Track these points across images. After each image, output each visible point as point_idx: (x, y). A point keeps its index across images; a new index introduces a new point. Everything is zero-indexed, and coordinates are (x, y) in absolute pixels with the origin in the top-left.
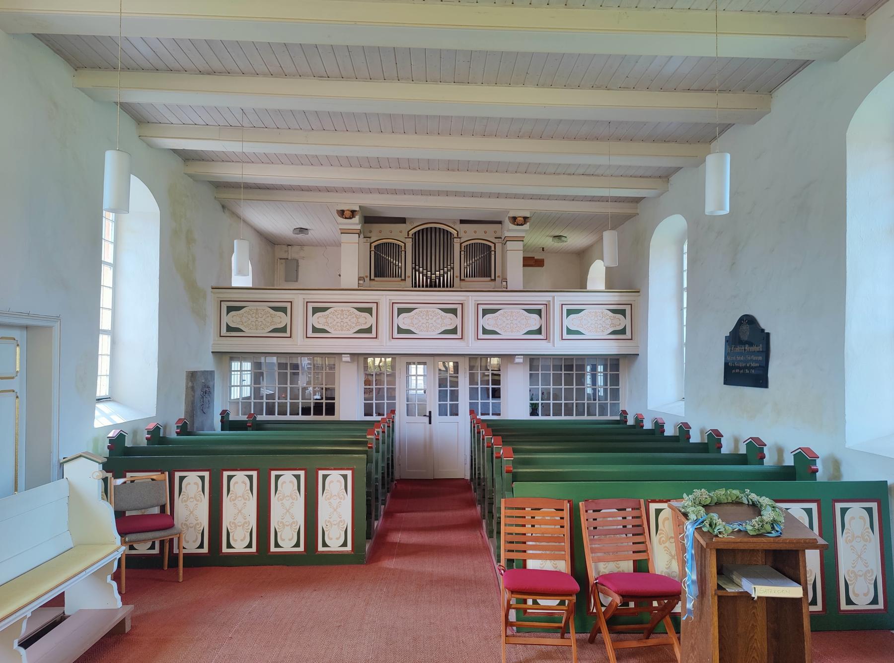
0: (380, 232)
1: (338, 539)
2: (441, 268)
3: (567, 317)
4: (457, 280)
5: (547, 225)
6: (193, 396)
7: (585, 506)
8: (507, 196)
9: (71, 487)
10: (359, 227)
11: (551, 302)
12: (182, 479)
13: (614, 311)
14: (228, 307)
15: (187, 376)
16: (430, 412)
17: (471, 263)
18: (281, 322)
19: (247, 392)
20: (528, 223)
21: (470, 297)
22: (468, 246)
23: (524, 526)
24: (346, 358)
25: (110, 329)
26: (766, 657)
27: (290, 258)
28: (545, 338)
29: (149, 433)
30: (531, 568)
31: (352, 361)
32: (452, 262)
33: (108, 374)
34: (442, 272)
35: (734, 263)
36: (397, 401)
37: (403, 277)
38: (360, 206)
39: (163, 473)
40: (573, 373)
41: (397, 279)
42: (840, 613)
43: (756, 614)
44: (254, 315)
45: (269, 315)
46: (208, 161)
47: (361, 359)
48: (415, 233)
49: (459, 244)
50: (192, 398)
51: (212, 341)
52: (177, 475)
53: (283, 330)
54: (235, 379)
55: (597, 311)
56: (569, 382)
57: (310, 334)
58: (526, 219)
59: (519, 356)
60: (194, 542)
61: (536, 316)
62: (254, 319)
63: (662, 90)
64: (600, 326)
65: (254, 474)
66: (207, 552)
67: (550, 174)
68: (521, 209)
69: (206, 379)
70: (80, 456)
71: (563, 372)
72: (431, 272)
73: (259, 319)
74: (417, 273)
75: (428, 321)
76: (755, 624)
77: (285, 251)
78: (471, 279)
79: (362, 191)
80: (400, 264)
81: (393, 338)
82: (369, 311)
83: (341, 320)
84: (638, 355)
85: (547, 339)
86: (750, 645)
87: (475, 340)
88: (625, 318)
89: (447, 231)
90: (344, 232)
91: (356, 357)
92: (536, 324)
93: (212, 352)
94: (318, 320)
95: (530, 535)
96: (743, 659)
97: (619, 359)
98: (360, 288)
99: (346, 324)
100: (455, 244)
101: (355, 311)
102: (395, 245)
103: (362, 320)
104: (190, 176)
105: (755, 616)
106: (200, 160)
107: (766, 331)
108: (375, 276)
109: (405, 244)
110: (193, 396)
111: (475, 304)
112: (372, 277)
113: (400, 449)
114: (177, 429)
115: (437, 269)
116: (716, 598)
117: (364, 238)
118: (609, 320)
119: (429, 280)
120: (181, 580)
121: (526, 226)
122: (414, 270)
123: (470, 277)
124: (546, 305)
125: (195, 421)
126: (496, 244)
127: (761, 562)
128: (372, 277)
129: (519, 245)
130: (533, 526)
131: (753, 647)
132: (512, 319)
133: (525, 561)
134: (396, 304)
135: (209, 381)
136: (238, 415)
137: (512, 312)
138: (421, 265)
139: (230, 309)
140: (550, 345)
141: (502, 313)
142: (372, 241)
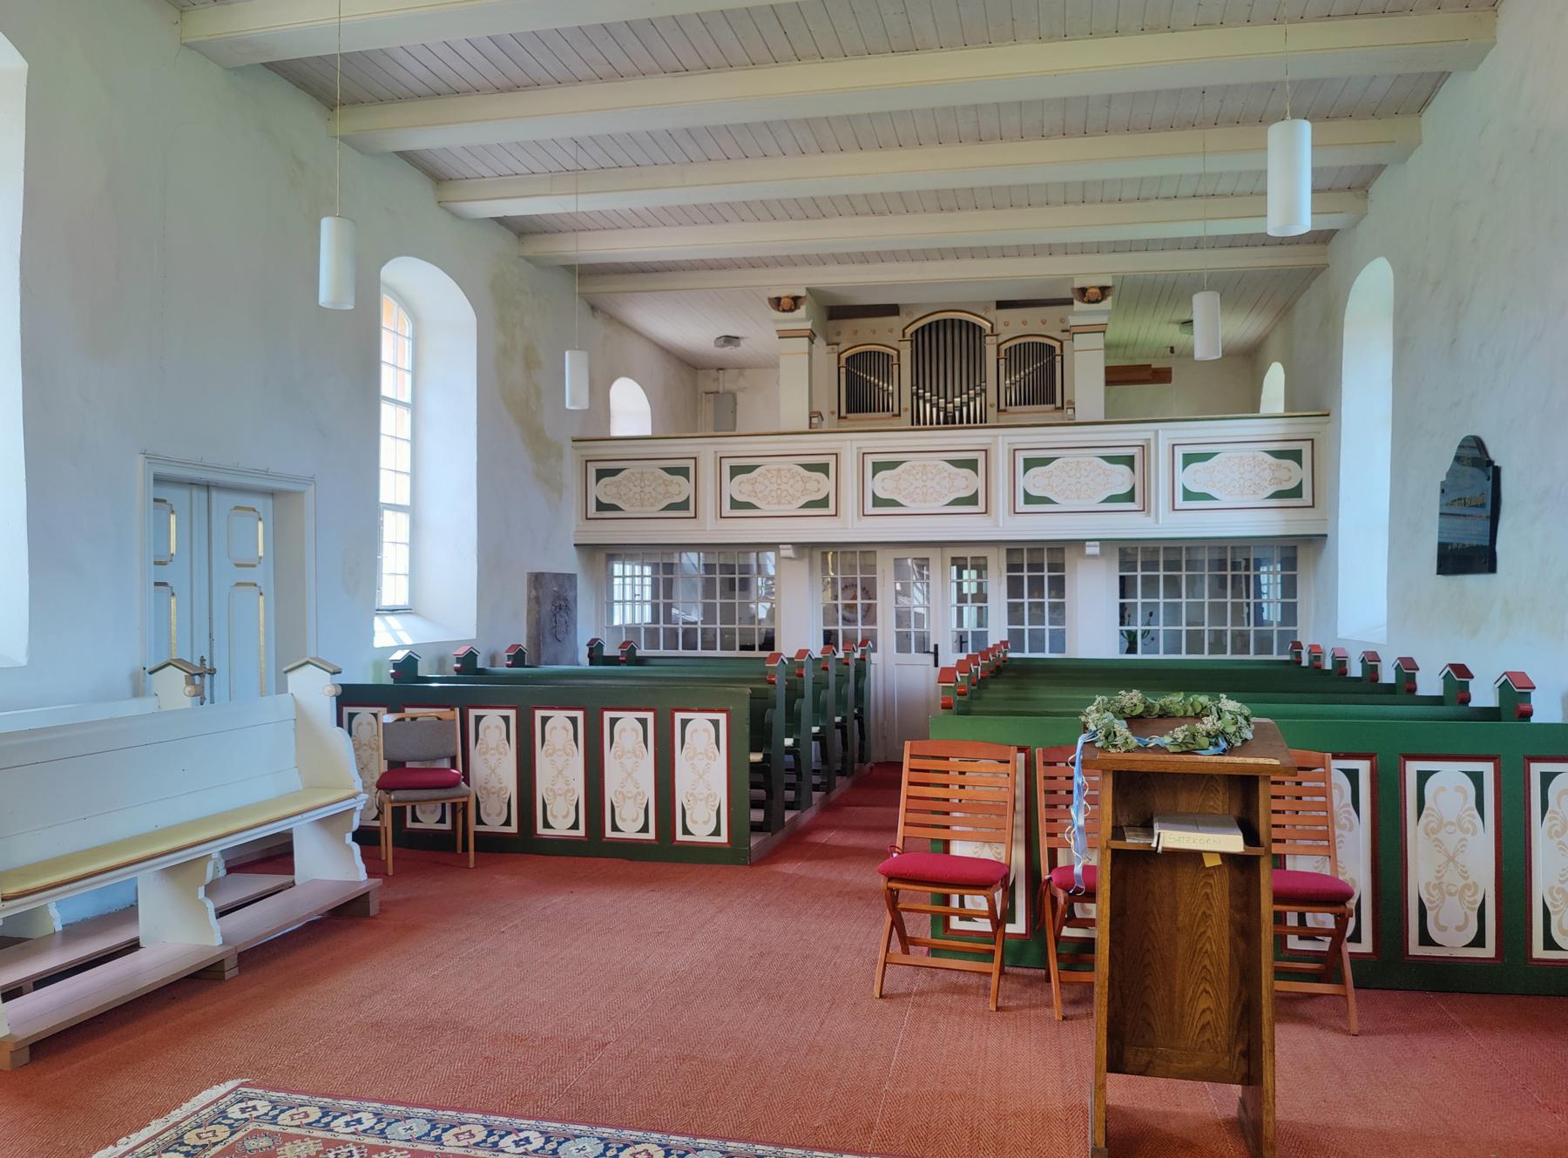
0: (856, 332)
1: (705, 823)
2: (964, 390)
3: (1183, 469)
4: (992, 412)
5: (1158, 300)
6: (539, 612)
7: (1044, 755)
8: (1067, 249)
9: (299, 709)
10: (808, 325)
11: (1152, 442)
12: (479, 719)
13: (1279, 454)
14: (598, 471)
15: (529, 580)
16: (936, 647)
17: (1018, 379)
18: (680, 493)
20: (1110, 299)
21: (1000, 438)
22: (1013, 350)
23: (947, 786)
24: (787, 552)
25: (409, 504)
26: (1227, 968)
27: (721, 391)
28: (1141, 509)
29: (458, 660)
30: (958, 855)
31: (799, 557)
32: (983, 380)
33: (407, 572)
34: (965, 396)
35: (1454, 340)
37: (896, 411)
38: (808, 289)
39: (452, 710)
41: (886, 414)
42: (1531, 963)
43: (1210, 896)
45: (660, 481)
46: (552, 232)
47: (817, 554)
48: (917, 331)
50: (537, 616)
51: (572, 527)
52: (473, 713)
53: (684, 505)
57: (727, 510)
58: (1104, 291)
59: (1092, 543)
60: (499, 814)
61: (1124, 469)
62: (639, 489)
63: (1276, 22)
65: (579, 715)
66: (516, 831)
67: (1130, 201)
68: (1093, 272)
69: (561, 586)
70: (308, 663)
72: (946, 398)
74: (921, 402)
76: (1208, 912)
78: (1018, 408)
79: (807, 260)
80: (890, 388)
81: (864, 515)
82: (824, 468)
83: (781, 487)
84: (1326, 536)
85: (1144, 510)
86: (1199, 947)
87: (1009, 515)
88: (1301, 467)
89: (974, 325)
90: (783, 335)
91: (806, 551)
93: (575, 545)
94: (739, 488)
95: (957, 801)
96: (1187, 969)
97: (1295, 547)
98: (811, 430)
101: (801, 470)
102: (881, 355)
103: (812, 486)
104: (528, 259)
105: (1208, 898)
106: (541, 233)
107: (1496, 464)
108: (849, 411)
109: (899, 352)
110: (539, 612)
111: (1009, 450)
112: (843, 413)
113: (885, 707)
114: (508, 660)
116: (1109, 853)
117: (828, 345)
118: (1268, 470)
119: (942, 414)
120: (472, 865)
121: (1107, 304)
122: (915, 397)
123: (1016, 404)
124: (1143, 446)
125: (542, 651)
126: (1065, 343)
127: (1220, 810)
128: (843, 413)
129: (1098, 340)
130: (962, 787)
131: (1204, 951)
132: (1078, 475)
133: (947, 843)
134: (869, 455)
135: (566, 590)
137: (1078, 462)
138: (927, 388)
139: (601, 474)
140: (1150, 520)
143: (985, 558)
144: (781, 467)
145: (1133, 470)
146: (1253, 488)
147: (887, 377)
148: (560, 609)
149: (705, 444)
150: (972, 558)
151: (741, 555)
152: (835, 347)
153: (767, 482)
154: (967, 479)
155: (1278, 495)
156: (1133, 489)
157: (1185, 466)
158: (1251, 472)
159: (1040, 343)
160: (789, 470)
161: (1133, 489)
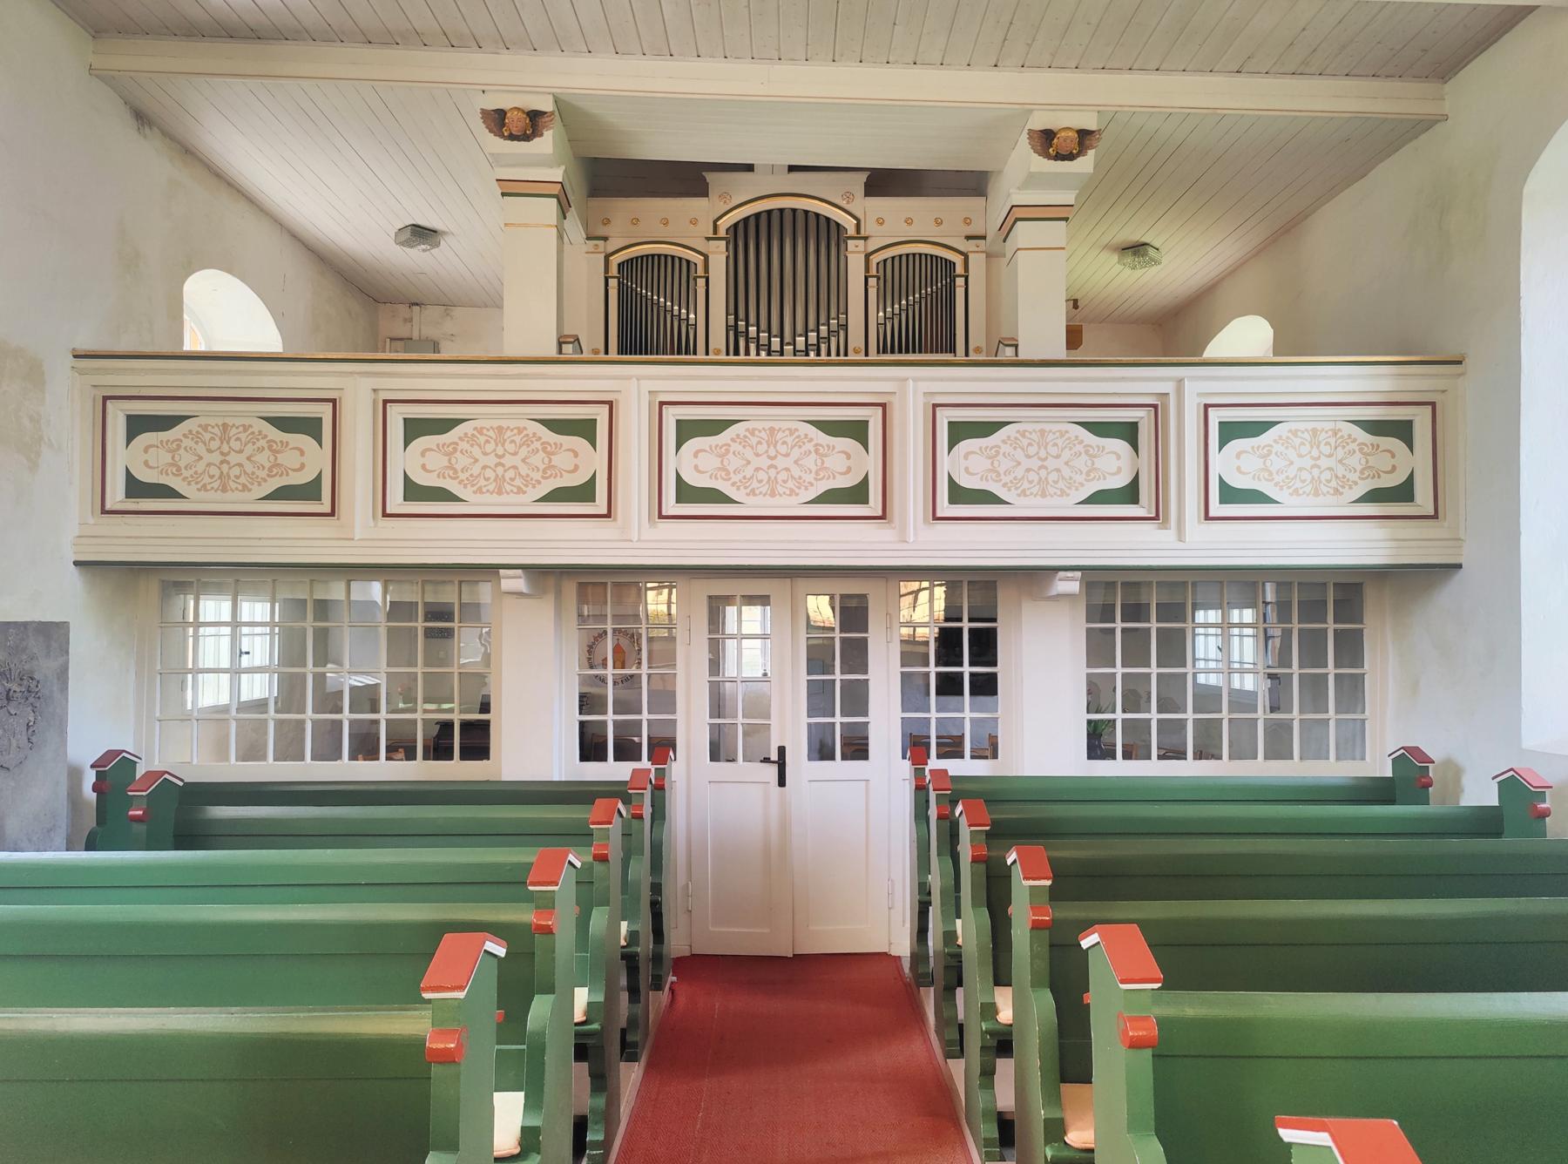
0: (635, 221)
2: (812, 325)
3: (1220, 450)
10: (557, 174)
13: (1376, 428)
14: (130, 418)
16: (782, 750)
17: (897, 311)
18: (303, 466)
19: (257, 687)
20: (1091, 153)
24: (514, 582)
27: (415, 336)
28: (1153, 515)
32: (842, 309)
34: (812, 336)
36: (680, 716)
38: (556, 101)
40: (1149, 629)
44: (215, 445)
45: (262, 443)
48: (736, 225)
49: (863, 256)
53: (310, 491)
54: (213, 649)
55: (1319, 426)
56: (1136, 651)
57: (396, 502)
58: (1085, 137)
59: (1070, 574)
61: (1120, 446)
64: (1327, 475)
71: (1119, 625)
73: (233, 458)
75: (770, 462)
77: (405, 320)
80: (692, 316)
81: (661, 516)
82: (585, 429)
85: (1156, 518)
89: (828, 219)
90: (511, 190)
91: (551, 581)
92: (1119, 470)
99: (511, 473)
100: (849, 255)
102: (677, 261)
103: (563, 460)
111: (925, 404)
115: (800, 329)
117: (588, 239)
118: (1358, 455)
121: (1085, 164)
122: (732, 334)
124: (1155, 407)
126: (971, 256)
136: (223, 755)
137: (1042, 432)
138: (752, 319)
139: (137, 426)
141: (1013, 435)
142: (610, 250)
143: (863, 598)
144: (504, 423)
145: (1135, 446)
146: (1334, 483)
147: (688, 300)
148: (8, 699)
149: (351, 373)
150: (842, 596)
151: (428, 588)
152: (601, 243)
153: (476, 451)
154: (849, 457)
155: (1374, 496)
156: (1135, 481)
157: (1222, 443)
158: (1330, 456)
159: (932, 256)
160: (520, 430)
161: (1135, 481)
